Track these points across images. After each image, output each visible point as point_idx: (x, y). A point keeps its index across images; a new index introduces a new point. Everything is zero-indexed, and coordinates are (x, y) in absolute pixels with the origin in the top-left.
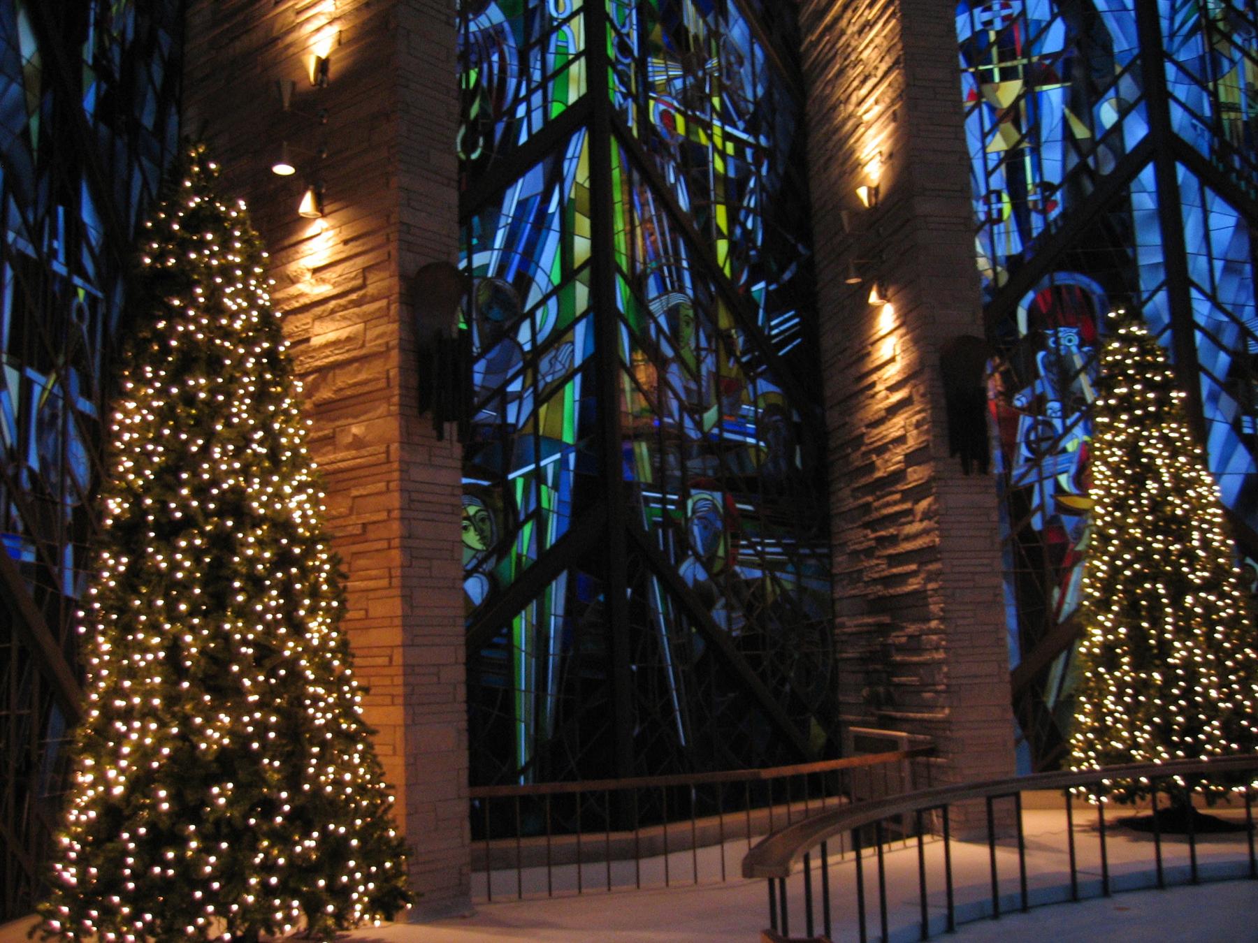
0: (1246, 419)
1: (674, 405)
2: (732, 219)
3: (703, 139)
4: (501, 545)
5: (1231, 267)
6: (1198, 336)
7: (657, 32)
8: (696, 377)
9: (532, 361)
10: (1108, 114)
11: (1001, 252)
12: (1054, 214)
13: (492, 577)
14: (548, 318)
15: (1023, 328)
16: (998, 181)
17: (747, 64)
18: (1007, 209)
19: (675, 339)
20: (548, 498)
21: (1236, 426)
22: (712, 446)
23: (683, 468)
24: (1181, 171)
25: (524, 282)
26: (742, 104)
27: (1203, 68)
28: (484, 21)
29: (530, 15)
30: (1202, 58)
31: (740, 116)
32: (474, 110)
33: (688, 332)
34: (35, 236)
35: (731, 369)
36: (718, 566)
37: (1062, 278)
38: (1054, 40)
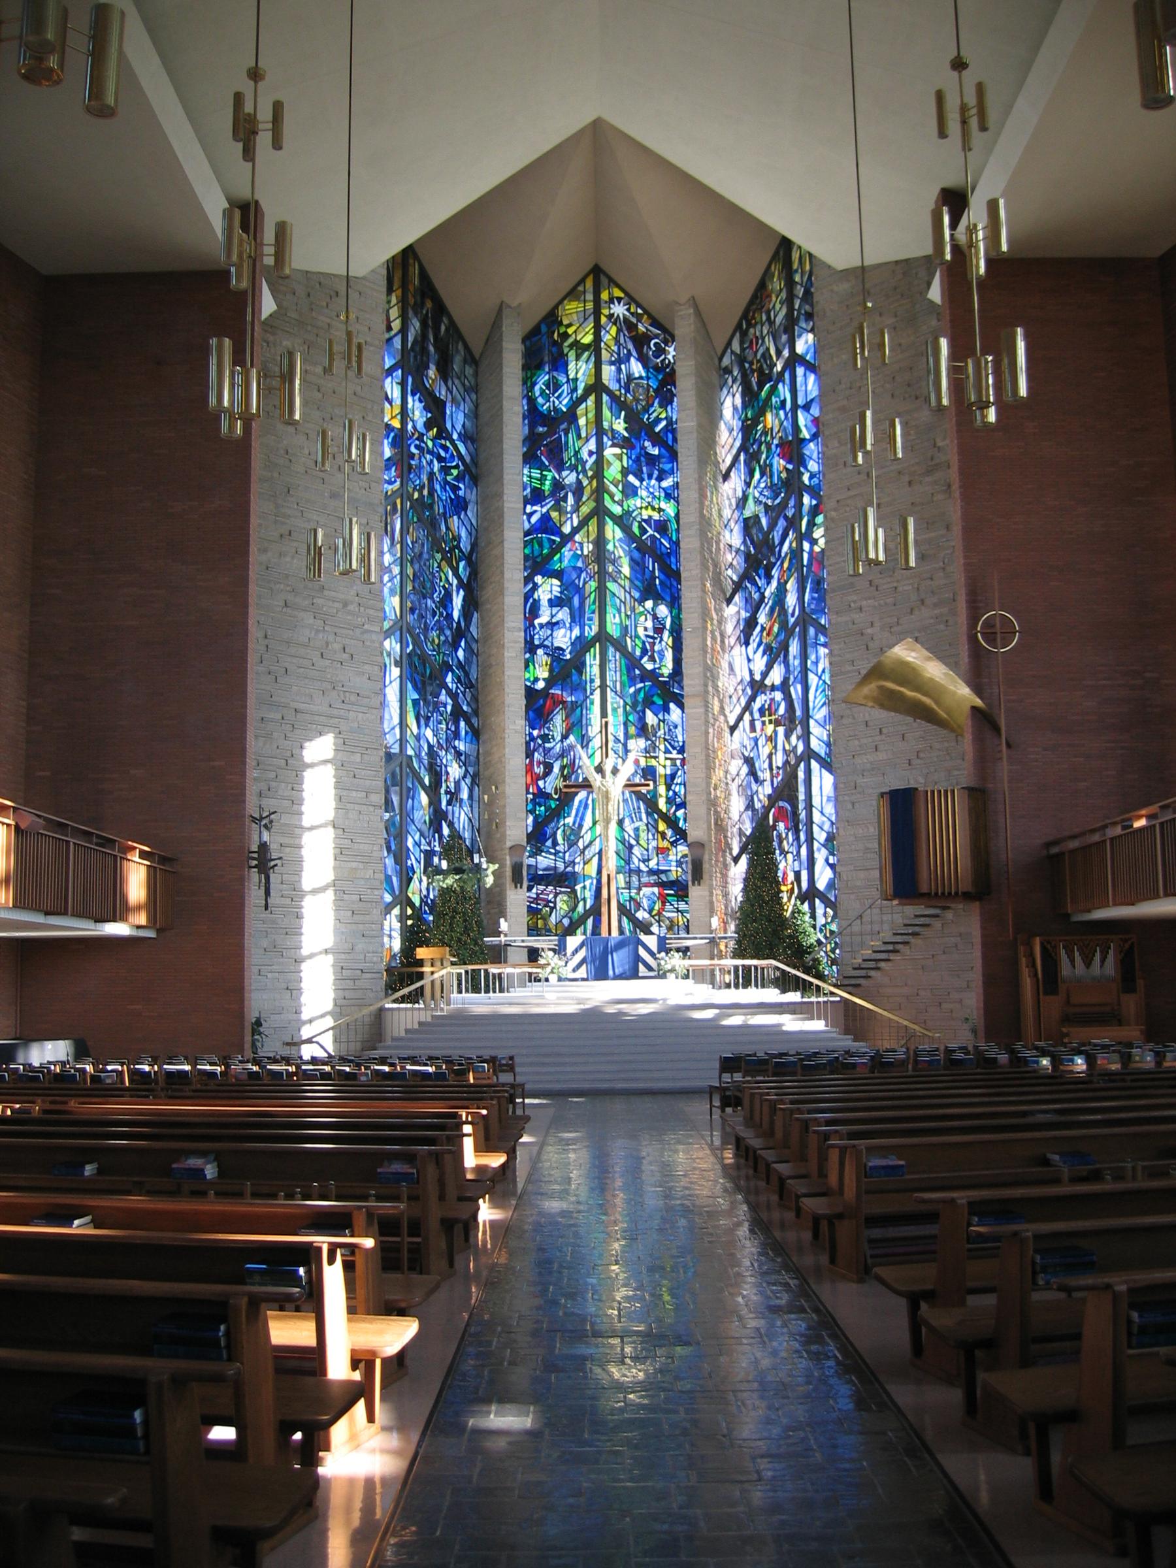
0: (831, 858)
1: (636, 860)
2: (668, 788)
3: (653, 762)
4: (574, 909)
5: (829, 799)
6: (814, 826)
7: (632, 730)
8: (647, 850)
9: (583, 852)
10: (793, 739)
11: (766, 793)
12: (780, 778)
13: (570, 918)
14: (587, 838)
15: (771, 823)
16: (766, 765)
17: (680, 728)
18: (767, 775)
19: (637, 839)
20: (588, 894)
21: (827, 860)
22: (651, 872)
23: (639, 880)
24: (813, 762)
25: (581, 826)
26: (676, 744)
27: (825, 721)
28: (568, 741)
29: (583, 736)
30: (825, 717)
31: (674, 748)
32: (565, 772)
33: (643, 835)
34: (429, 844)
35: (665, 844)
36: (654, 912)
37: (781, 804)
38: (782, 711)
